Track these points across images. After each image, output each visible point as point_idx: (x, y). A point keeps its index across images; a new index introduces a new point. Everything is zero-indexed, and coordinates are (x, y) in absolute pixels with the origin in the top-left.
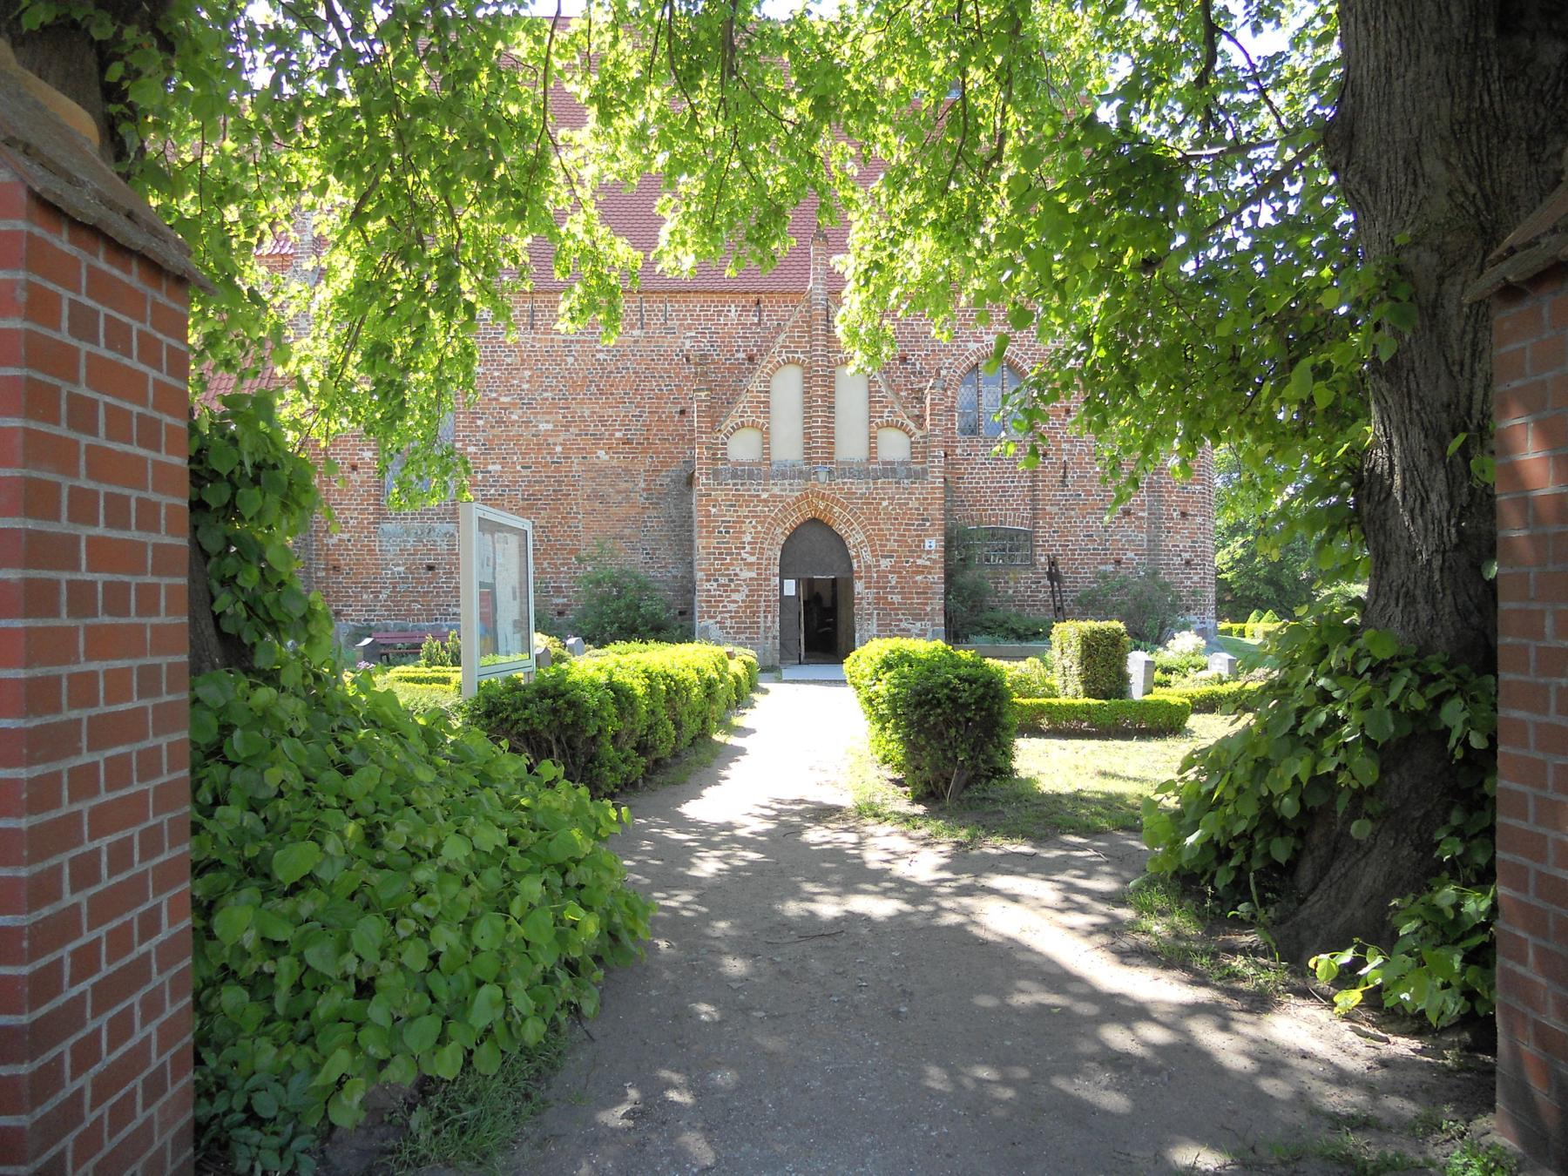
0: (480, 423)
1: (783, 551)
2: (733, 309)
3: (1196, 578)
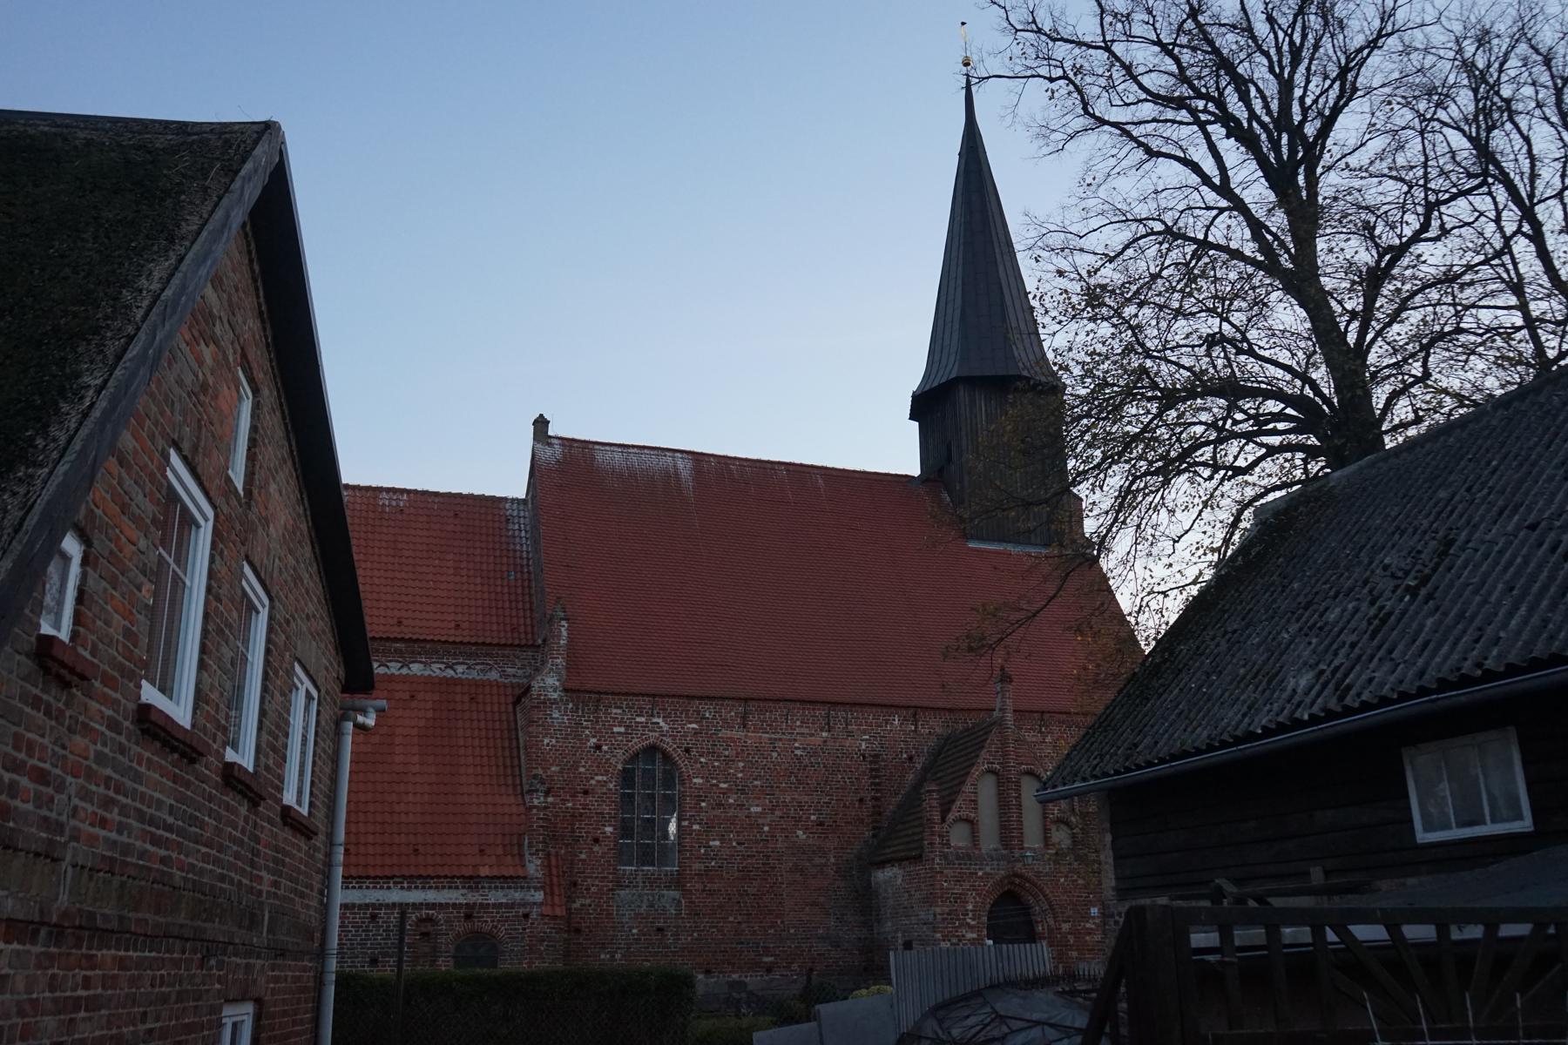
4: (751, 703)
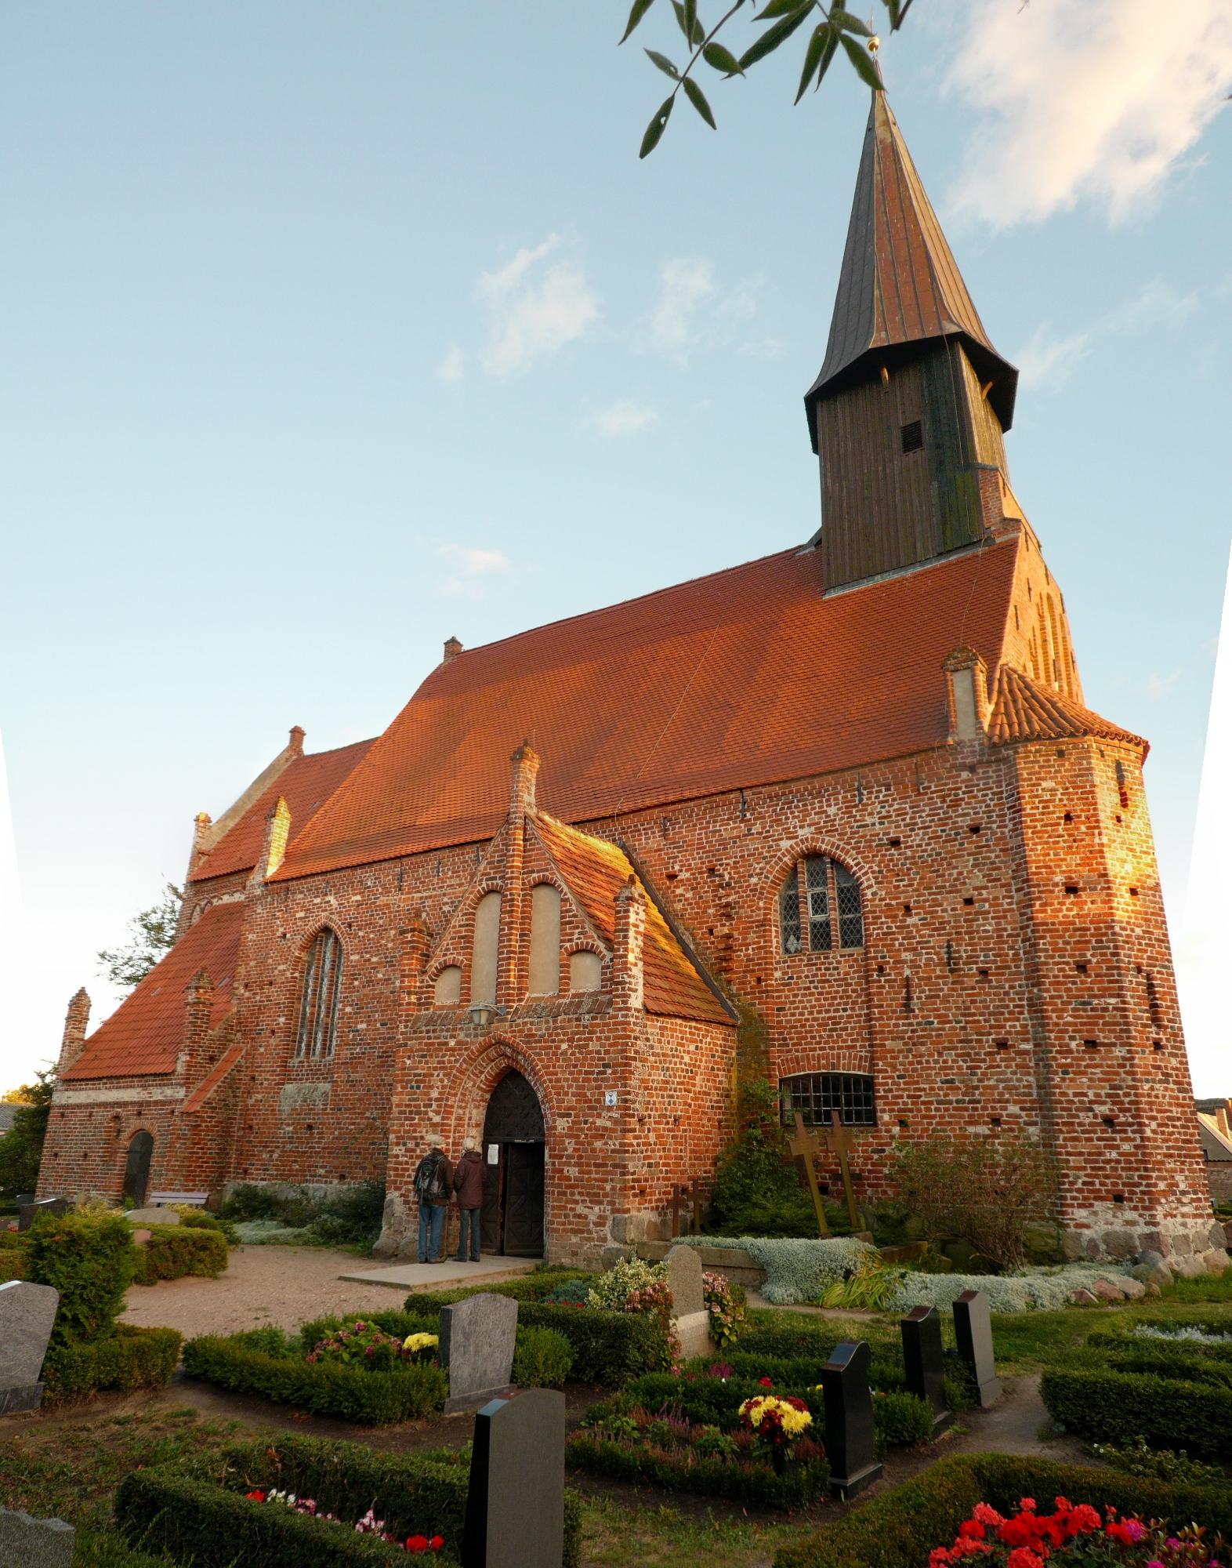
0: (356, 983)
3: (1126, 1147)
4: (405, 861)
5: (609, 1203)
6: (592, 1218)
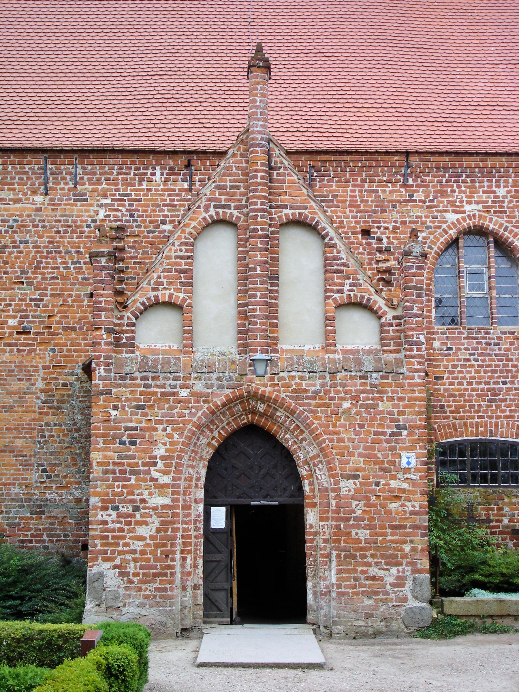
1: (210, 469)
2: (158, 172)
5: (408, 564)
6: (389, 579)
